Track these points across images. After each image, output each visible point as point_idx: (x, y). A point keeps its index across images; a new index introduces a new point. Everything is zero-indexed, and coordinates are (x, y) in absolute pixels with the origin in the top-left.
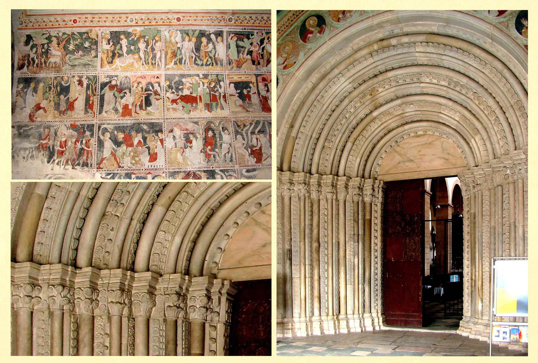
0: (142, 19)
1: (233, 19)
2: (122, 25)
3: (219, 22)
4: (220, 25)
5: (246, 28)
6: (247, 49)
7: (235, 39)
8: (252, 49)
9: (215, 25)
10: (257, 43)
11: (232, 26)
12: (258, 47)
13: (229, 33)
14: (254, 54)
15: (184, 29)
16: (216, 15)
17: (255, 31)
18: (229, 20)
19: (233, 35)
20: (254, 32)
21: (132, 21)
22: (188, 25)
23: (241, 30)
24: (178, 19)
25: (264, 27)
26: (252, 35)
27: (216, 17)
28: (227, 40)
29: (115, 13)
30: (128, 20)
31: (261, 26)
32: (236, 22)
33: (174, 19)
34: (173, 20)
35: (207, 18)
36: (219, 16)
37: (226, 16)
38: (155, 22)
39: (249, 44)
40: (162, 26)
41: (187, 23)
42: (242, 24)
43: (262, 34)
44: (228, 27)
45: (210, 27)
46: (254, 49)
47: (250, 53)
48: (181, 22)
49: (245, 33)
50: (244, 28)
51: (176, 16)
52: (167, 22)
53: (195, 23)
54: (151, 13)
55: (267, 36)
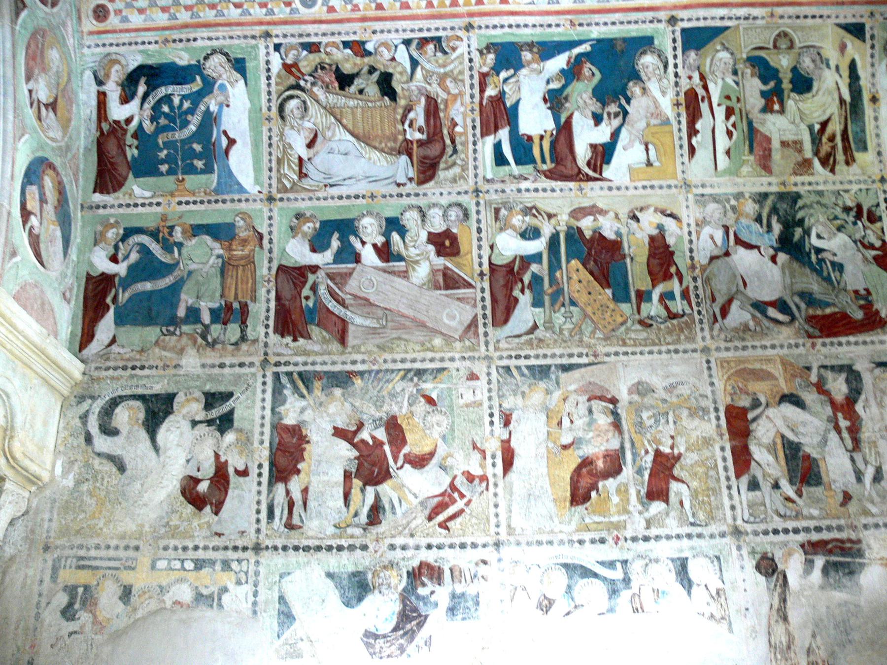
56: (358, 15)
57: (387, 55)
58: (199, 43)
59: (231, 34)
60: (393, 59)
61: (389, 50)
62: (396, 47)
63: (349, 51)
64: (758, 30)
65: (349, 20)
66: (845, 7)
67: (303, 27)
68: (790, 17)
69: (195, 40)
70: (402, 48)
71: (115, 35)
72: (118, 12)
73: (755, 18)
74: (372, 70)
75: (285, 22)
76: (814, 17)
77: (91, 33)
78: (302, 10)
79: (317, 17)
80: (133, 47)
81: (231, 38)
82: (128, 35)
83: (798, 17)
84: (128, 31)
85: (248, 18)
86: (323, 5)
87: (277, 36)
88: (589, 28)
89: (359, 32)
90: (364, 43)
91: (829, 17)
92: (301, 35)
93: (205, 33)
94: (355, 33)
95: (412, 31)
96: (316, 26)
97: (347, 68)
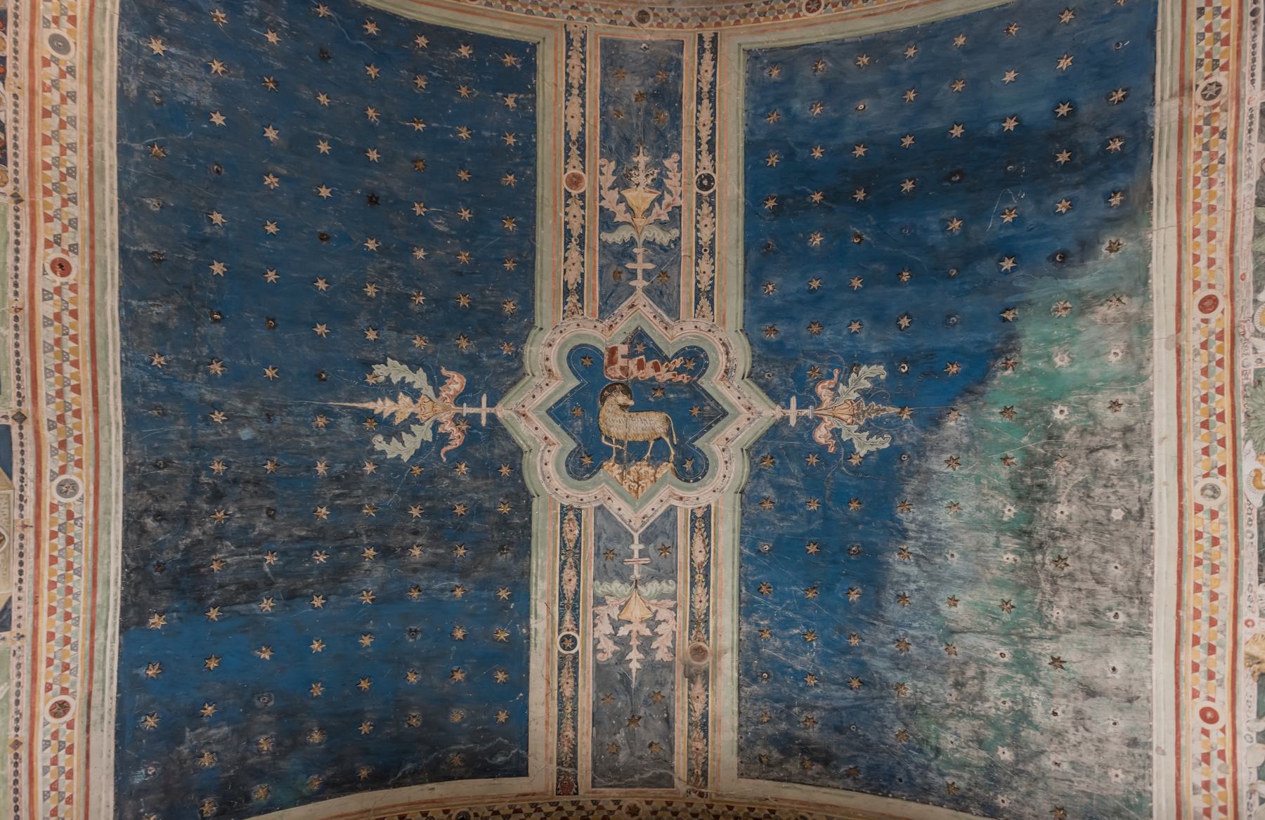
0: (1206, 451)
2: (1230, 532)
3: (1223, 135)
15: (1250, 278)
21: (1216, 491)
22: (1231, 260)
24: (1208, 304)
27: (1198, 155)
29: (1180, 553)
30: (1208, 504)
32: (1222, 62)
33: (1205, 321)
34: (1212, 325)
35: (1204, 191)
36: (1193, 145)
37: (1195, 115)
38: (1218, 397)
40: (1239, 369)
41: (1226, 265)
45: (1243, 169)
48: (1221, 293)
50: (1248, 19)
51: (1194, 315)
52: (1221, 349)
53: (1223, 234)
54: (1179, 416)
64: (6, 511)
66: (31, 606)
68: (21, 546)
73: (21, 507)
76: (21, 572)
83: (21, 555)
88: (12, 327)
91: (20, 589)
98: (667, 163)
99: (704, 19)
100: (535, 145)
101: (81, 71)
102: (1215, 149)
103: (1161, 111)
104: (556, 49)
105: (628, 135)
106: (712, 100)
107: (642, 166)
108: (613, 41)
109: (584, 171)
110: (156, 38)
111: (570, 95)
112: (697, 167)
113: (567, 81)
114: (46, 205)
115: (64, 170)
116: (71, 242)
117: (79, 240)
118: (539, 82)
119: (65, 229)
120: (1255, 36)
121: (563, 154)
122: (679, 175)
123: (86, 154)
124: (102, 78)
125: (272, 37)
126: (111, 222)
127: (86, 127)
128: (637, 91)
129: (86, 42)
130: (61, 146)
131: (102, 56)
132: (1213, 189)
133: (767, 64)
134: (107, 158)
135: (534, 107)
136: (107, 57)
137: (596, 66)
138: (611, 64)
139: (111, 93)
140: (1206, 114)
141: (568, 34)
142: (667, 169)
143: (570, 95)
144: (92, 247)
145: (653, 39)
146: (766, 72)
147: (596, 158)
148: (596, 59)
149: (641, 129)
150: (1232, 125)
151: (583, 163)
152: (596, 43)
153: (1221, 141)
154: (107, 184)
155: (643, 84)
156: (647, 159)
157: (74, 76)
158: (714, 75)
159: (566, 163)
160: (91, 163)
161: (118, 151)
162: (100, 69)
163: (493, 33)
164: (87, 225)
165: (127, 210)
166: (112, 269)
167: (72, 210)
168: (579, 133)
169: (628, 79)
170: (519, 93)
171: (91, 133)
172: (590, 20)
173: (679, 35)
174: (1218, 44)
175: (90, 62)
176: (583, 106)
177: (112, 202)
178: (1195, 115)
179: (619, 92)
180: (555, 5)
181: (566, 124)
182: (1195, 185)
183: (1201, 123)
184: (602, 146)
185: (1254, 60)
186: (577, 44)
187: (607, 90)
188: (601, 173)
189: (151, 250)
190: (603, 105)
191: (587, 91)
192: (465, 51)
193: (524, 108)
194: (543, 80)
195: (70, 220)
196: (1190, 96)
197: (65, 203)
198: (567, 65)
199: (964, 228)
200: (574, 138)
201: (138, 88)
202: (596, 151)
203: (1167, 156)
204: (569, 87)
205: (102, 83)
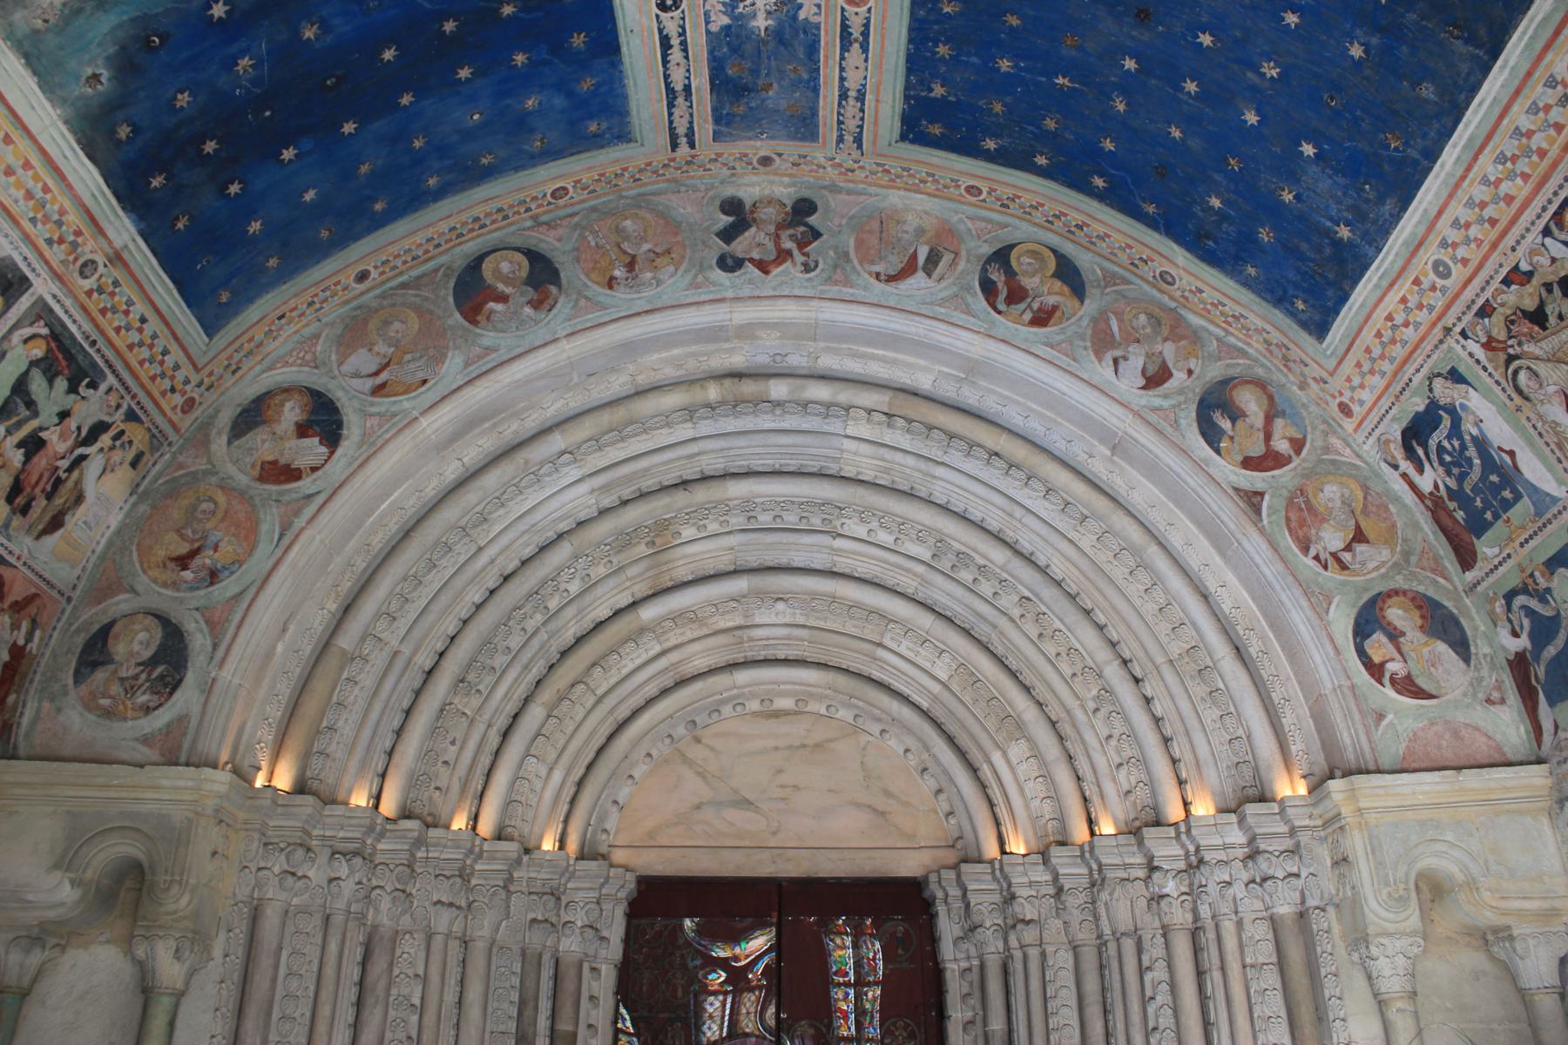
1: (96, 276)
3: (49, 242)
4: (41, 255)
5: (101, 343)
6: (34, 424)
7: (38, 352)
8: (51, 436)
9: (27, 237)
10: (79, 428)
11: (71, 293)
12: (70, 442)
13: (42, 312)
14: (41, 461)
16: (67, 204)
17: (111, 379)
18: (85, 265)
19: (45, 331)
20: (104, 377)
23: (79, 337)
25: (143, 386)
26: (93, 385)
28: (15, 327)
31: (136, 377)
35: (30, 184)
36: (74, 218)
37: (91, 244)
39: (57, 409)
42: (100, 318)
43: (118, 407)
44: (55, 288)
46: (55, 438)
47: (34, 445)
49: (80, 358)
50: (95, 336)
55: (122, 426)
56: (1486, 247)
57: (1545, 261)
58: (1416, 380)
59: (1426, 352)
60: (1554, 260)
61: (1543, 256)
62: (1543, 245)
63: (1514, 287)
65: (1485, 258)
67: (1462, 297)
69: (1410, 380)
70: (1548, 241)
71: (1368, 420)
72: (1352, 399)
74: (1548, 287)
75: (1448, 307)
77: (1356, 430)
78: (1447, 283)
79: (1463, 279)
80: (1385, 420)
81: (1429, 356)
82: (1374, 413)
84: (1370, 410)
85: (1423, 329)
86: (1455, 264)
87: (1454, 325)
89: (1503, 261)
90: (1516, 268)
92: (1469, 307)
93: (1410, 369)
94: (1501, 266)
95: (1539, 217)
96: (1469, 288)
97: (1530, 304)
98: (726, 20)
99: (688, 163)
100: (910, 41)
101: (1434, 240)
102: (48, 226)
103: (127, 230)
104: (875, 136)
105: (782, 48)
106: (670, 91)
107: (761, 16)
108: (803, 139)
109: (843, 10)
110: (1341, 239)
111: (859, 91)
112: (683, 19)
113: (863, 104)
114: (1552, 141)
115: (1509, 164)
116: (1550, 91)
117: (1540, 89)
118: (899, 106)
119: (1547, 108)
120: (80, 327)
121: (872, 29)
122: (708, 7)
123: (1476, 169)
124: (1416, 226)
125: (1216, 202)
126: (1488, 92)
127: (1459, 192)
128: (770, 93)
129: (1415, 261)
130: (1496, 188)
131: (1405, 243)
132: (22, 192)
133: (604, 133)
134: (1455, 156)
135: (907, 81)
136: (1400, 241)
137: (825, 117)
138: (804, 119)
139: (1415, 211)
140: (80, 249)
141: (860, 147)
142: (724, 13)
143: (859, 91)
144: (1529, 74)
145: (752, 142)
146: (604, 125)
147: (826, 23)
148: (825, 124)
149: (764, 55)
150: (47, 254)
151: (844, 18)
152: (824, 138)
153: (47, 236)
154: (1469, 132)
155: (763, 101)
156: (754, 24)
157: (1444, 239)
158: (670, 114)
159: (868, 19)
160: (1475, 158)
161: (1438, 158)
162: (1413, 234)
163: (953, 156)
164: (1520, 100)
165: (1463, 96)
166: (1520, 39)
167: (1525, 123)
168: (848, 51)
169: (783, 104)
170: (926, 98)
171: (1457, 186)
172: (832, 159)
173: (718, 147)
174: (109, 306)
175: (1421, 244)
176: (842, 79)
177: (1476, 112)
178: (91, 244)
179: (794, 92)
180: (873, 173)
181: (866, 60)
182: (45, 184)
183: (80, 240)
184: (818, 36)
185: (66, 312)
186: (849, 138)
187: (810, 94)
188: (818, 6)
189: (1459, 43)
190: (816, 79)
191: (837, 94)
192: (991, 144)
193: (921, 82)
194: (893, 107)
195: (1536, 114)
196: (106, 255)
197: (1529, 134)
198: (862, 119)
199: (297, 33)
200: (856, 46)
201: (1383, 205)
202: (826, 31)
203: (93, 195)
204: (861, 97)
205: (1419, 222)
